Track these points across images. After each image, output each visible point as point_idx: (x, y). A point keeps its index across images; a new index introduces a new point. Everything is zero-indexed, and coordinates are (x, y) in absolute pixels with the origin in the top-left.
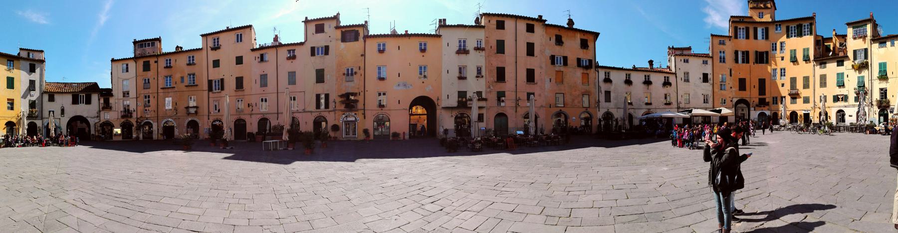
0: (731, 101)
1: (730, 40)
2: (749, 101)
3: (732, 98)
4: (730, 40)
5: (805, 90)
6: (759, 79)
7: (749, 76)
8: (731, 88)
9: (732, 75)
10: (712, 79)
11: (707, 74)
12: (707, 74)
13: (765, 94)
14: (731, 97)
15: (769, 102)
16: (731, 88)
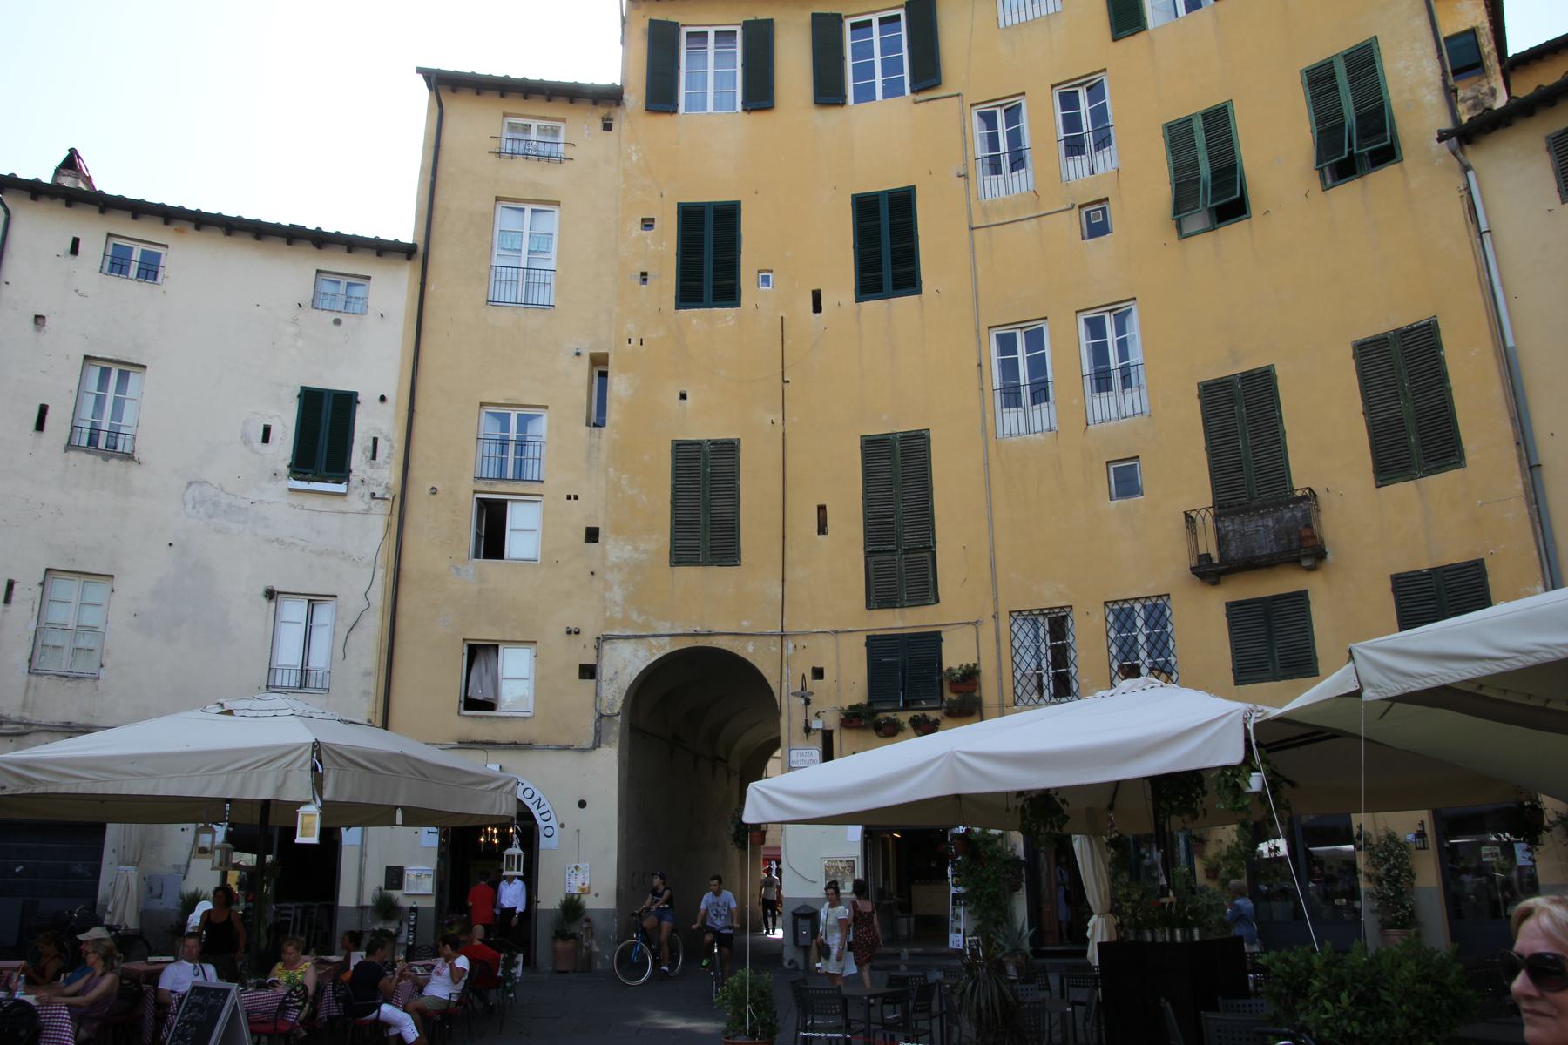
0: (588, 672)
1: (608, 127)
2: (768, 671)
3: (602, 640)
4: (608, 127)
5: (1402, 490)
6: (874, 448)
7: (766, 416)
8: (592, 535)
9: (612, 414)
10: (391, 449)
11: (345, 403)
12: (345, 403)
13: (924, 589)
14: (588, 636)
15: (970, 676)
16: (592, 535)
